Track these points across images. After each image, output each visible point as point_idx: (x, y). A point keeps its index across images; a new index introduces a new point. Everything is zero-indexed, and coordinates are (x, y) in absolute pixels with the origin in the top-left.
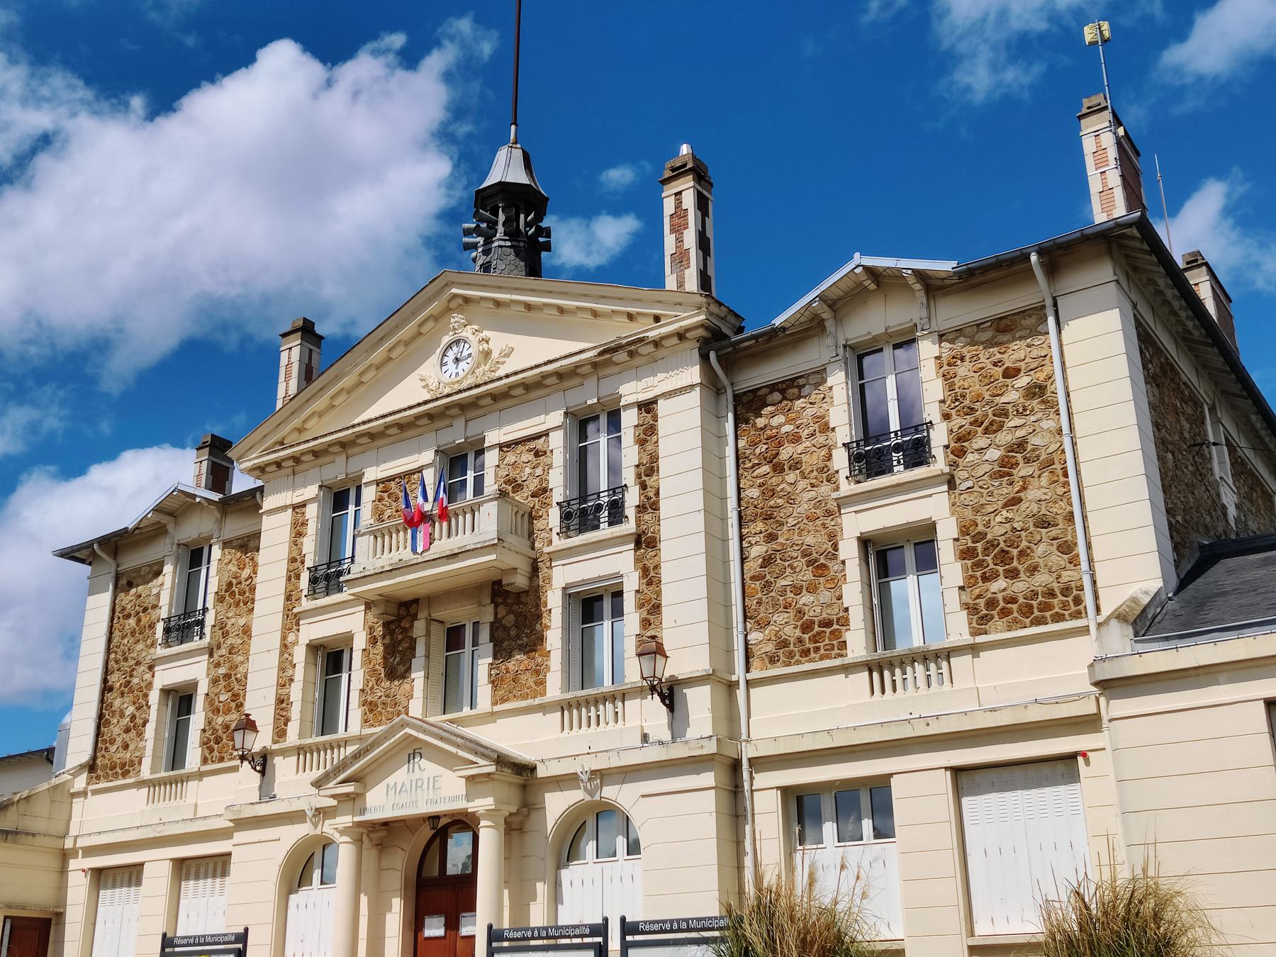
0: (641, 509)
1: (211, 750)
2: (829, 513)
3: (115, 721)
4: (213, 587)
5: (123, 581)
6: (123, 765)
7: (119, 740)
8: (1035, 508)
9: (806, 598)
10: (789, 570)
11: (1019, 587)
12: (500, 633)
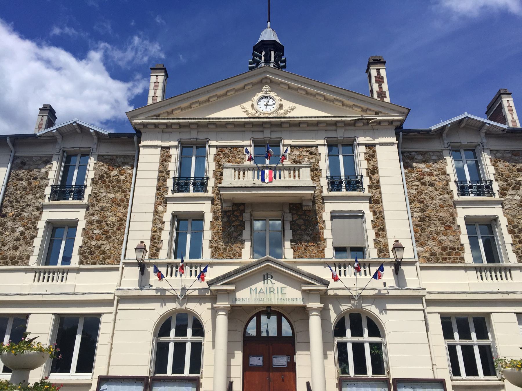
0: (370, 187)
1: (86, 258)
2: (450, 206)
3: (8, 233)
5: (19, 161)
6: (13, 258)
7: (10, 244)
9: (443, 237)
10: (432, 225)
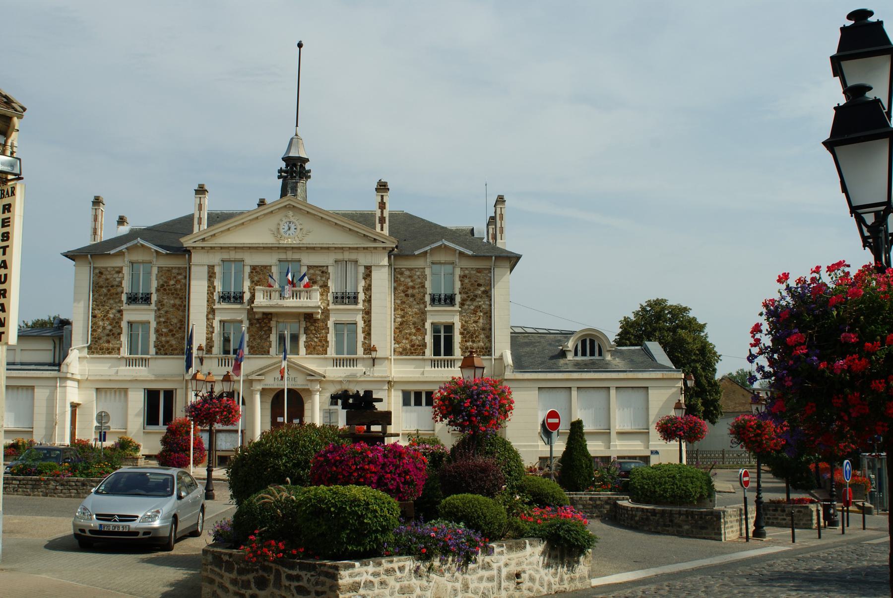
0: (364, 301)
1: (160, 350)
4: (154, 284)
5: (97, 271)
7: (105, 338)
9: (414, 338)
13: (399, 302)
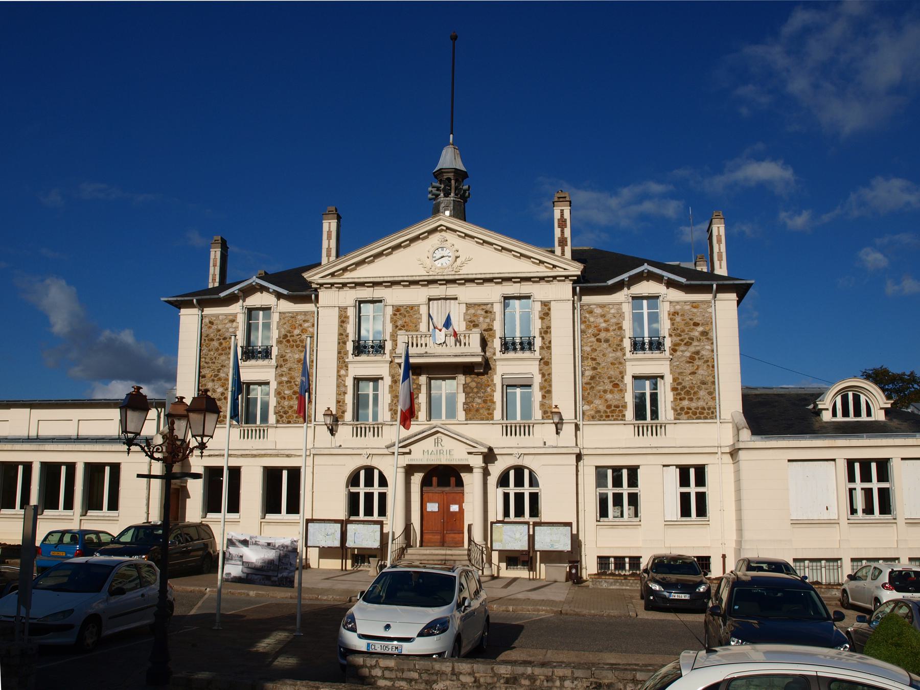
0: (542, 348)
1: (281, 417)
4: (275, 334)
5: (206, 320)
8: (700, 377)
11: (693, 405)
12: (468, 390)
13: (588, 349)
